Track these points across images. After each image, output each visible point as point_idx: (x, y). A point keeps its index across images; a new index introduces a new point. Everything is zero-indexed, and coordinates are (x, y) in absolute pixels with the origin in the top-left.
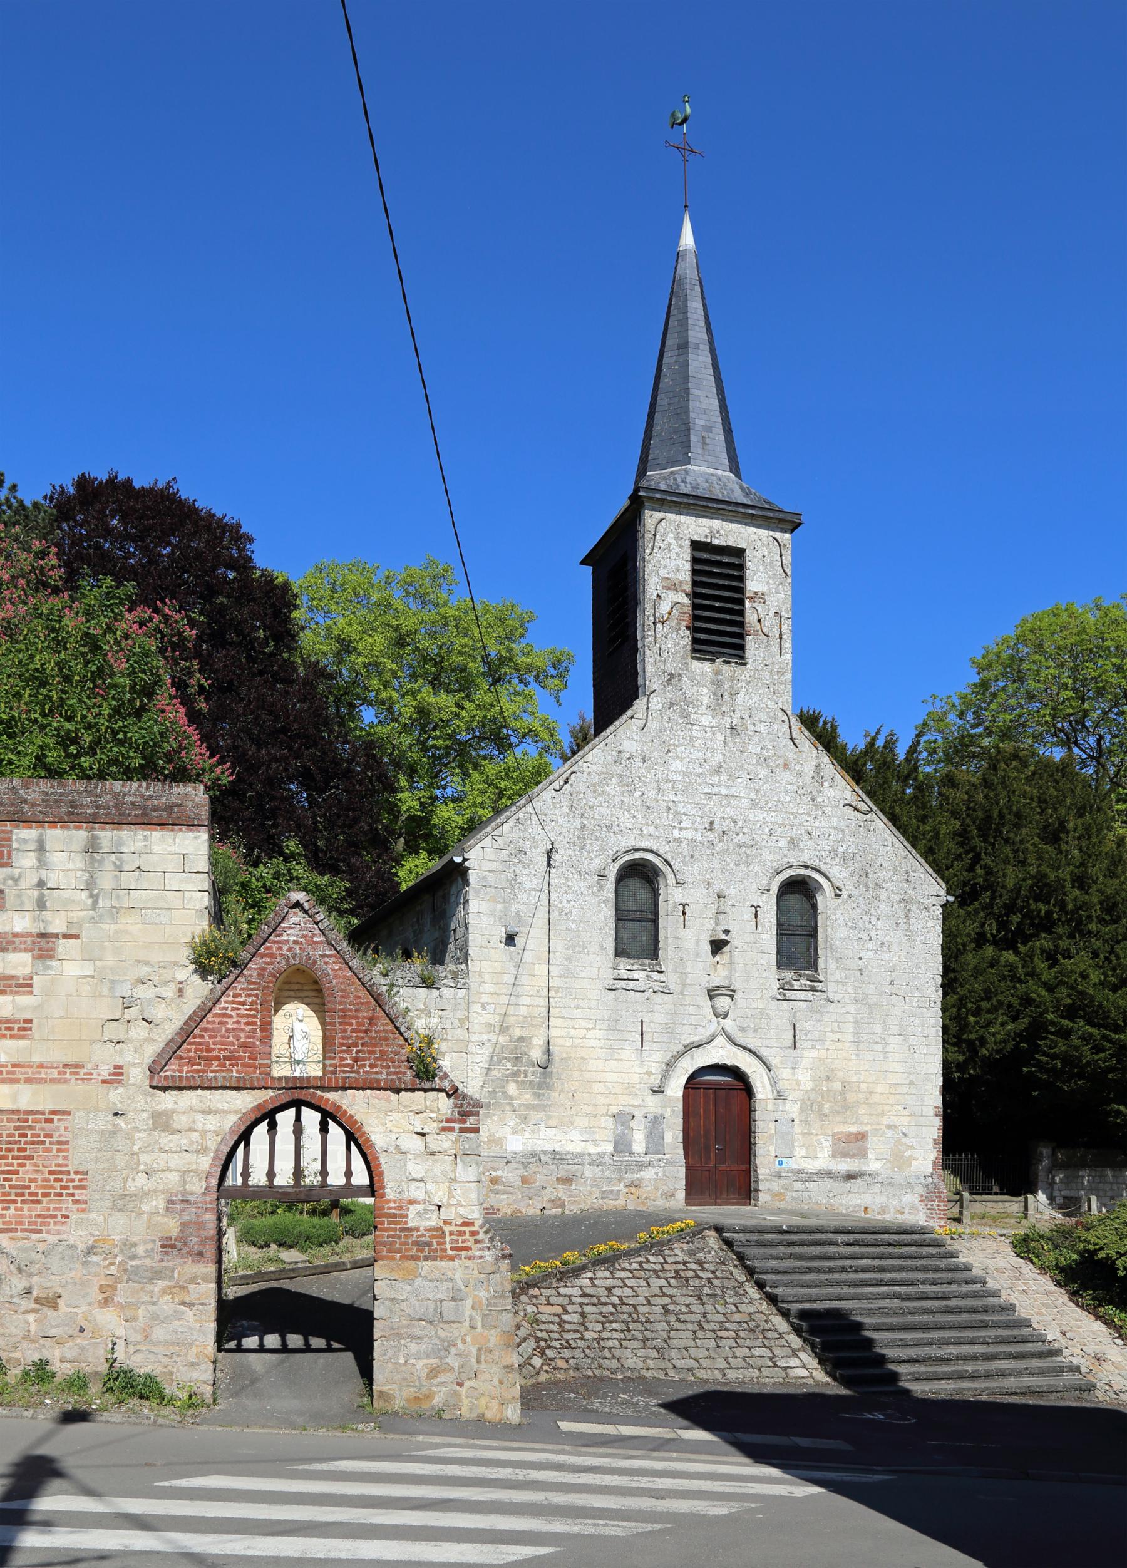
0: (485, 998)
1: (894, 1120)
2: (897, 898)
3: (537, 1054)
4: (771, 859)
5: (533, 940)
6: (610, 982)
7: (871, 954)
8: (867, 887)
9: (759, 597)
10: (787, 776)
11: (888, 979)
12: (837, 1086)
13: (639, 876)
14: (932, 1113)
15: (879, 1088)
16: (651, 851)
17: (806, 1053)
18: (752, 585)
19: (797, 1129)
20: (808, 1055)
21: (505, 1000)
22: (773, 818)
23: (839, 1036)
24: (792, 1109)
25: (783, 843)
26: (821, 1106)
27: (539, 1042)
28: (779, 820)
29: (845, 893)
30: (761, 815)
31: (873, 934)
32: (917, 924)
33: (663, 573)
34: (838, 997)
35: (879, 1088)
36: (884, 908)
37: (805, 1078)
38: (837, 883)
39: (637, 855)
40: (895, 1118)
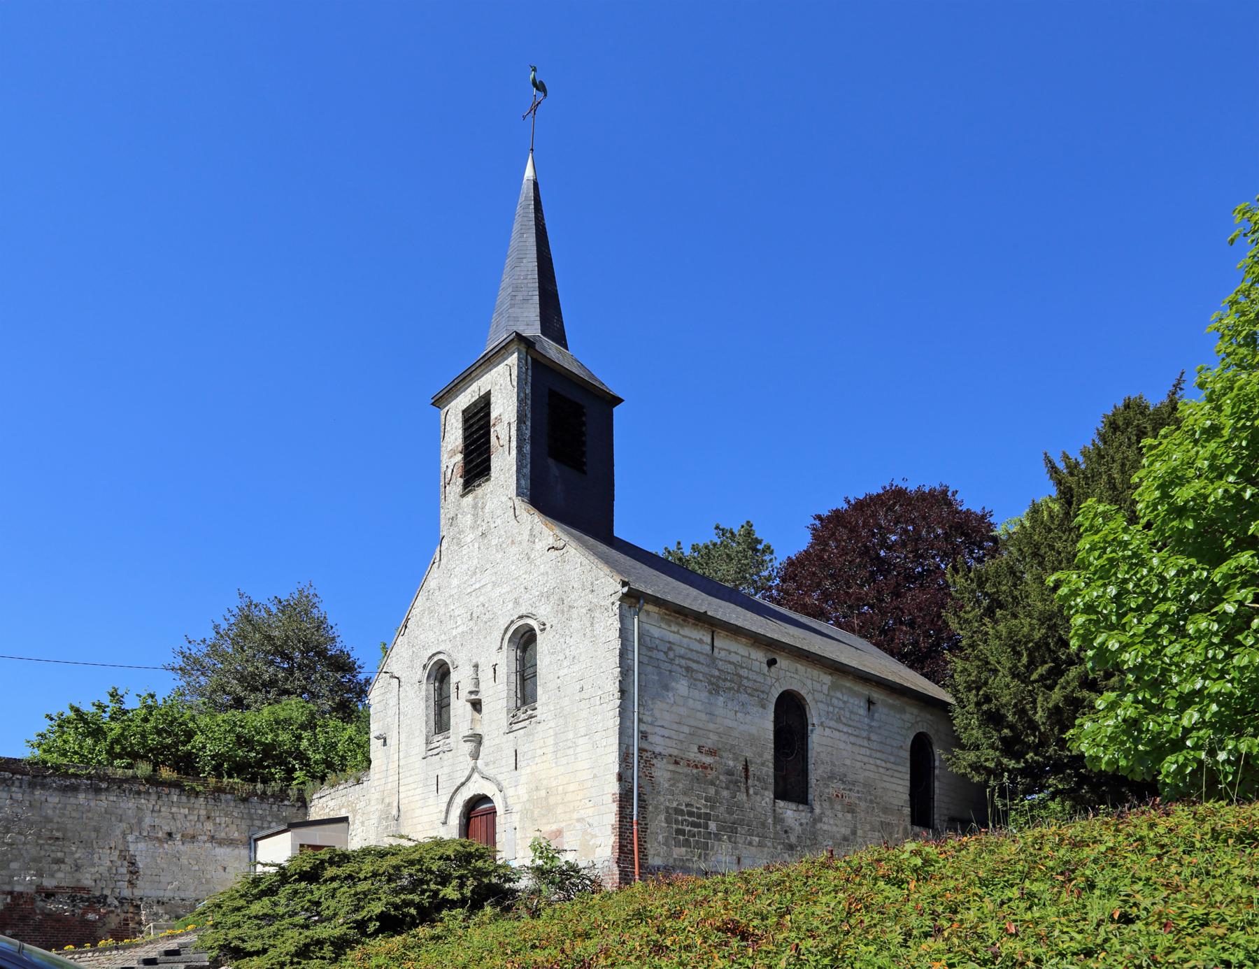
0: (376, 783)
1: (582, 813)
2: (584, 611)
3: (395, 812)
4: (503, 623)
5: (392, 741)
6: (423, 755)
7: (566, 671)
8: (563, 612)
9: (499, 419)
10: (514, 549)
11: (578, 687)
12: (543, 793)
13: (440, 673)
14: (610, 800)
15: (572, 787)
16: (434, 655)
17: (523, 772)
18: (493, 415)
19: (519, 835)
20: (524, 771)
21: (383, 781)
22: (506, 589)
23: (544, 750)
24: (515, 819)
25: (511, 605)
26: (533, 812)
27: (395, 804)
28: (508, 589)
29: (548, 626)
30: (498, 590)
31: (567, 653)
32: (599, 628)
33: (449, 448)
34: (544, 717)
35: (572, 787)
36: (575, 624)
37: (522, 791)
38: (543, 620)
39: (436, 659)
40: (582, 812)
